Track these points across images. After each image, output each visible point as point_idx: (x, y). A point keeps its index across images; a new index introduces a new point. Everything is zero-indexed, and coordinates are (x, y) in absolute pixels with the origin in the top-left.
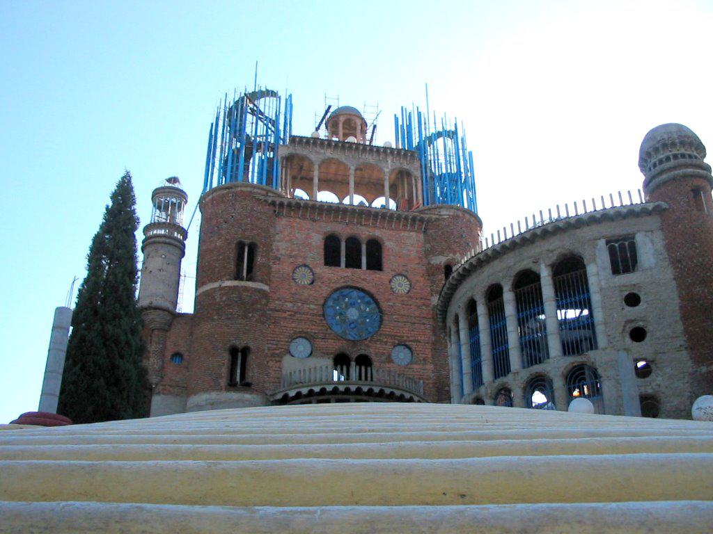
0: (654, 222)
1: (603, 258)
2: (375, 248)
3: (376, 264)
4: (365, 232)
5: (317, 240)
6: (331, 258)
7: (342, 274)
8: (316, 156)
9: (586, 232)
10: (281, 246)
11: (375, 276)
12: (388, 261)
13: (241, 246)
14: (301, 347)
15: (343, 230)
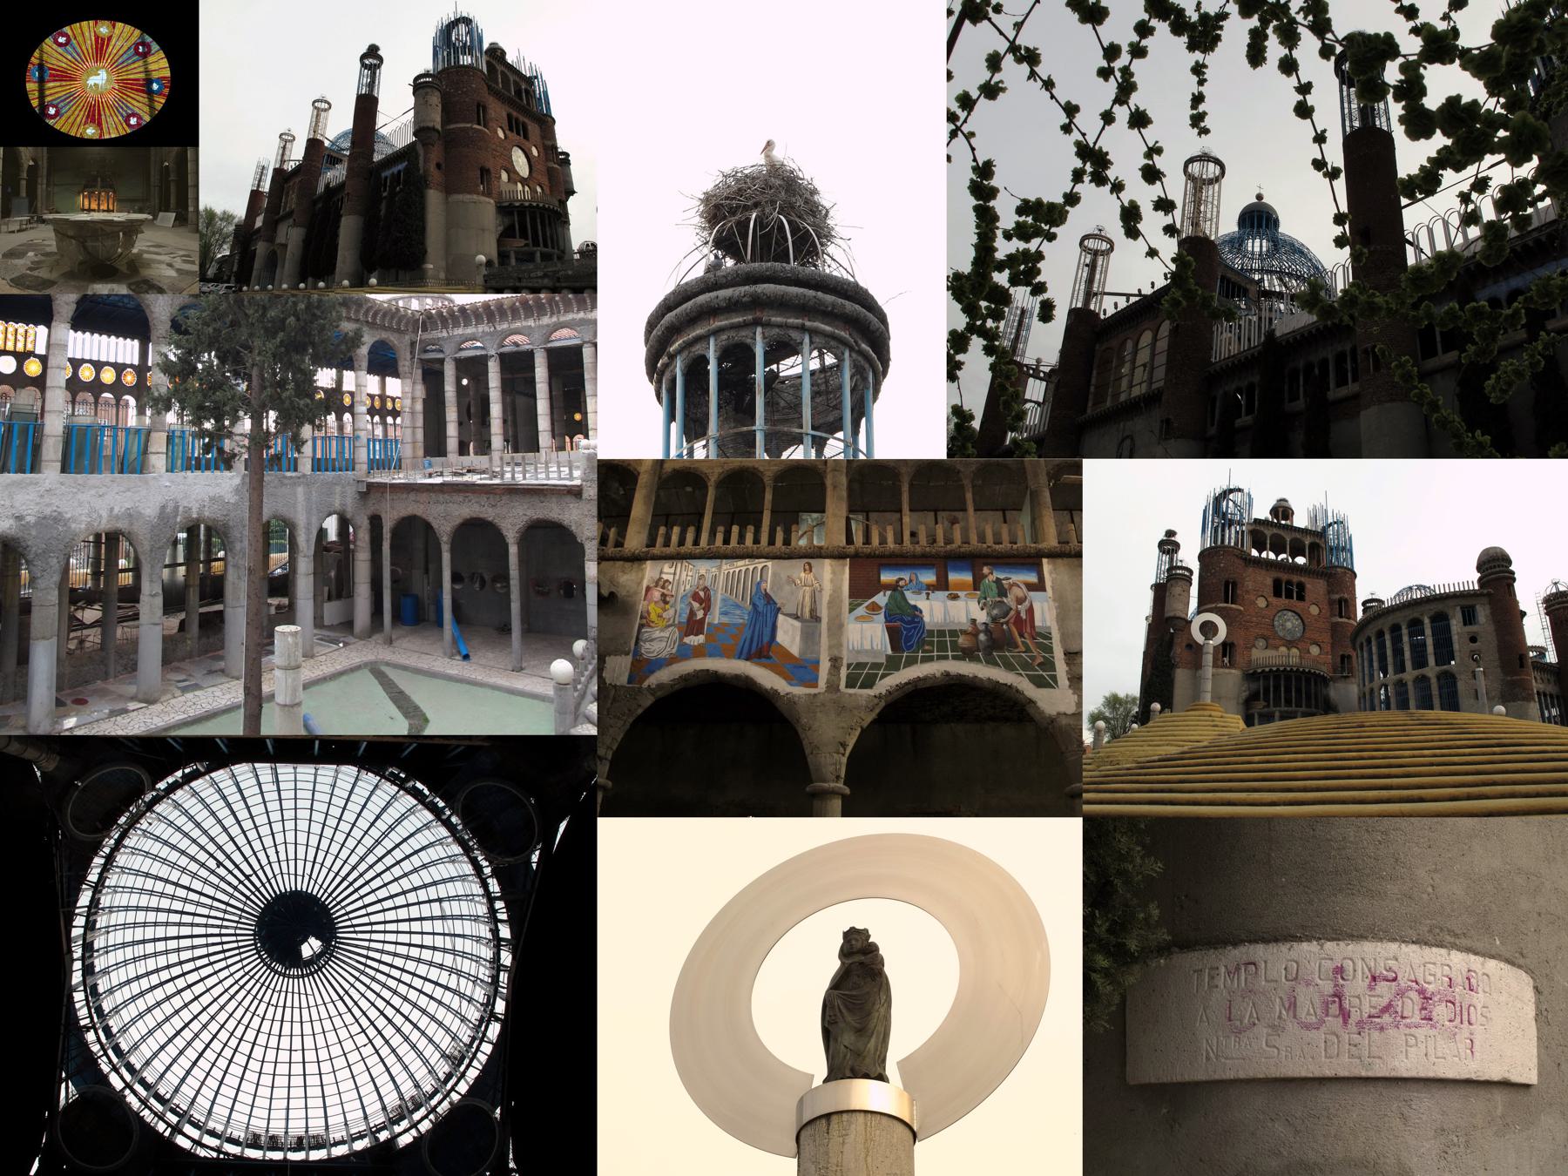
0: (1485, 600)
1: (1459, 615)
2: (1301, 587)
3: (1301, 598)
4: (1295, 578)
5: (1269, 581)
6: (1277, 593)
7: (1283, 601)
8: (1268, 532)
9: (1451, 603)
10: (1249, 585)
11: (1300, 604)
12: (1308, 595)
13: (1227, 584)
14: (1261, 643)
15: (1284, 577)
